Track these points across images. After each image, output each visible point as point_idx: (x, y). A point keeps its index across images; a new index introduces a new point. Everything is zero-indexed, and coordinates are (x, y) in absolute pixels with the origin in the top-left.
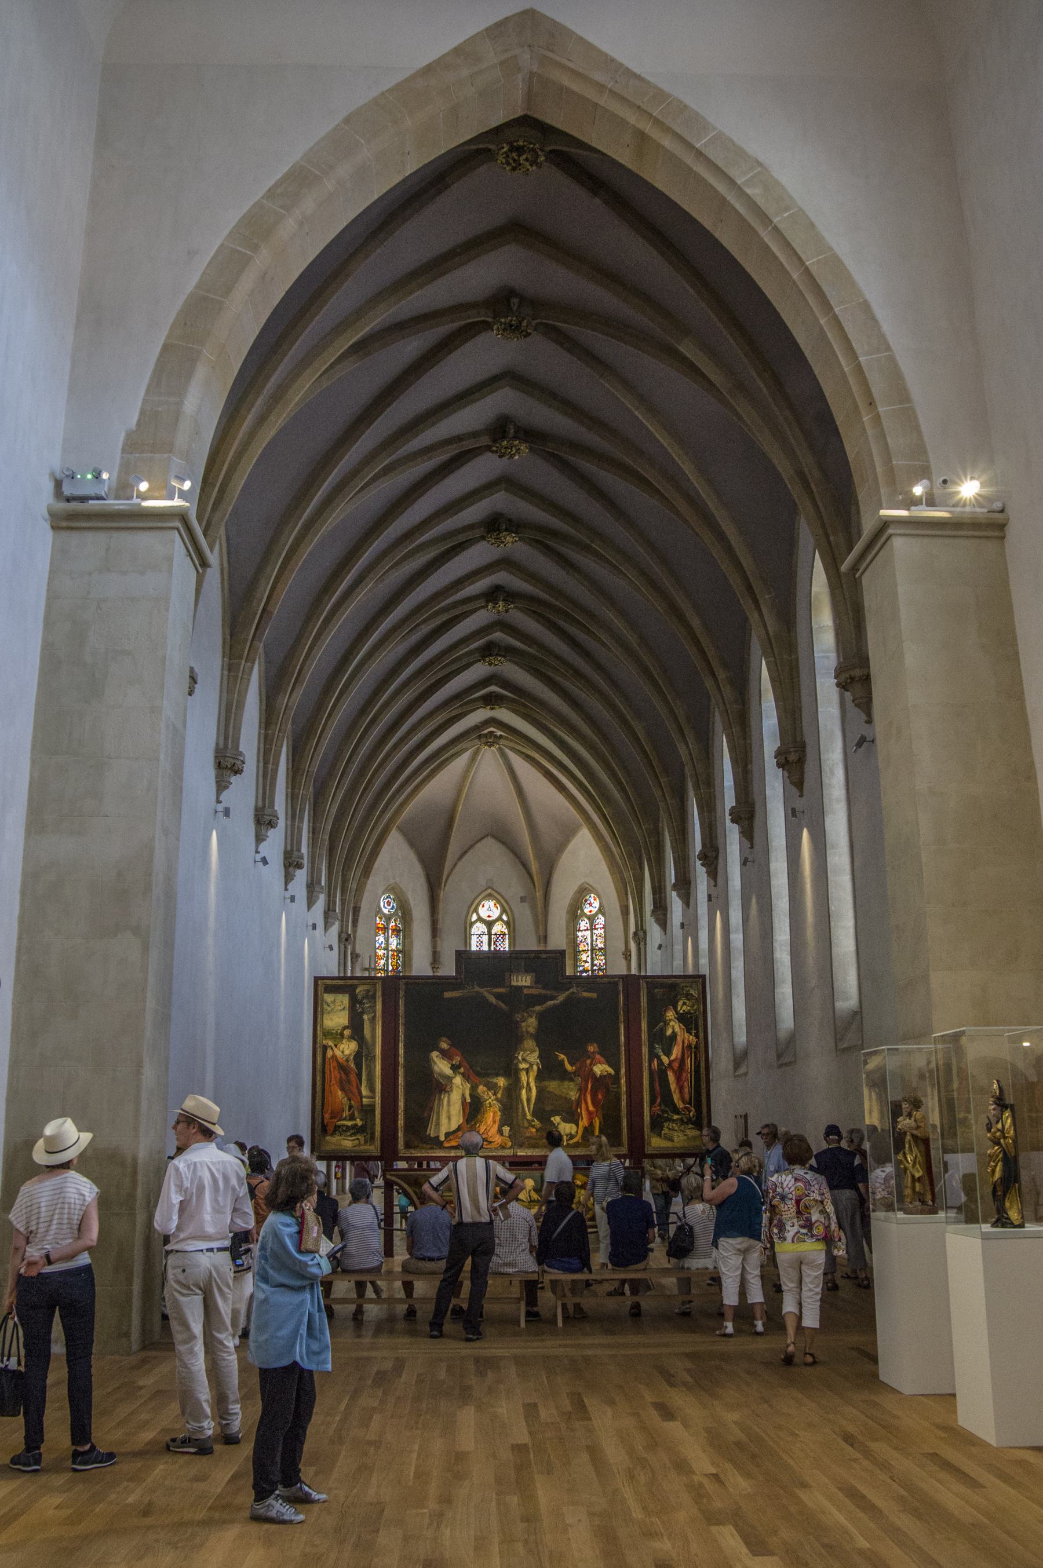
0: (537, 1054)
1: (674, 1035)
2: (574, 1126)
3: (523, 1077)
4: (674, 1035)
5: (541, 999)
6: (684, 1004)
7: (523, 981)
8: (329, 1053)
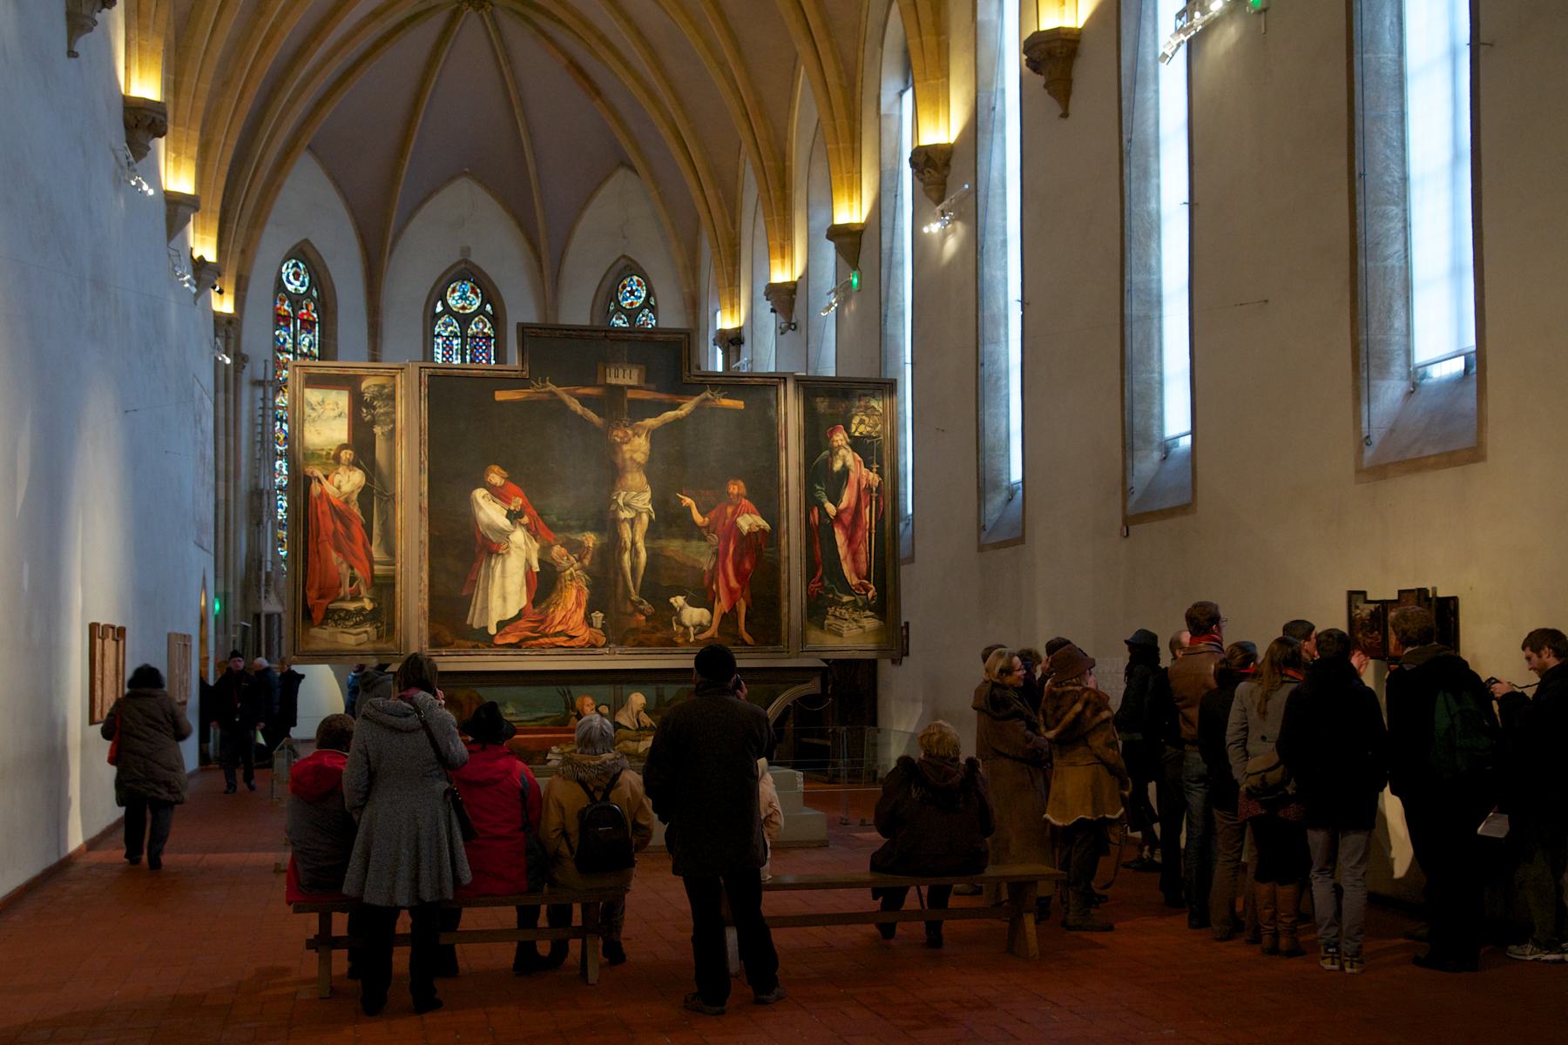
0: (648, 496)
1: (845, 471)
2: (705, 612)
4: (845, 471)
5: (657, 408)
6: (862, 422)
8: (315, 489)
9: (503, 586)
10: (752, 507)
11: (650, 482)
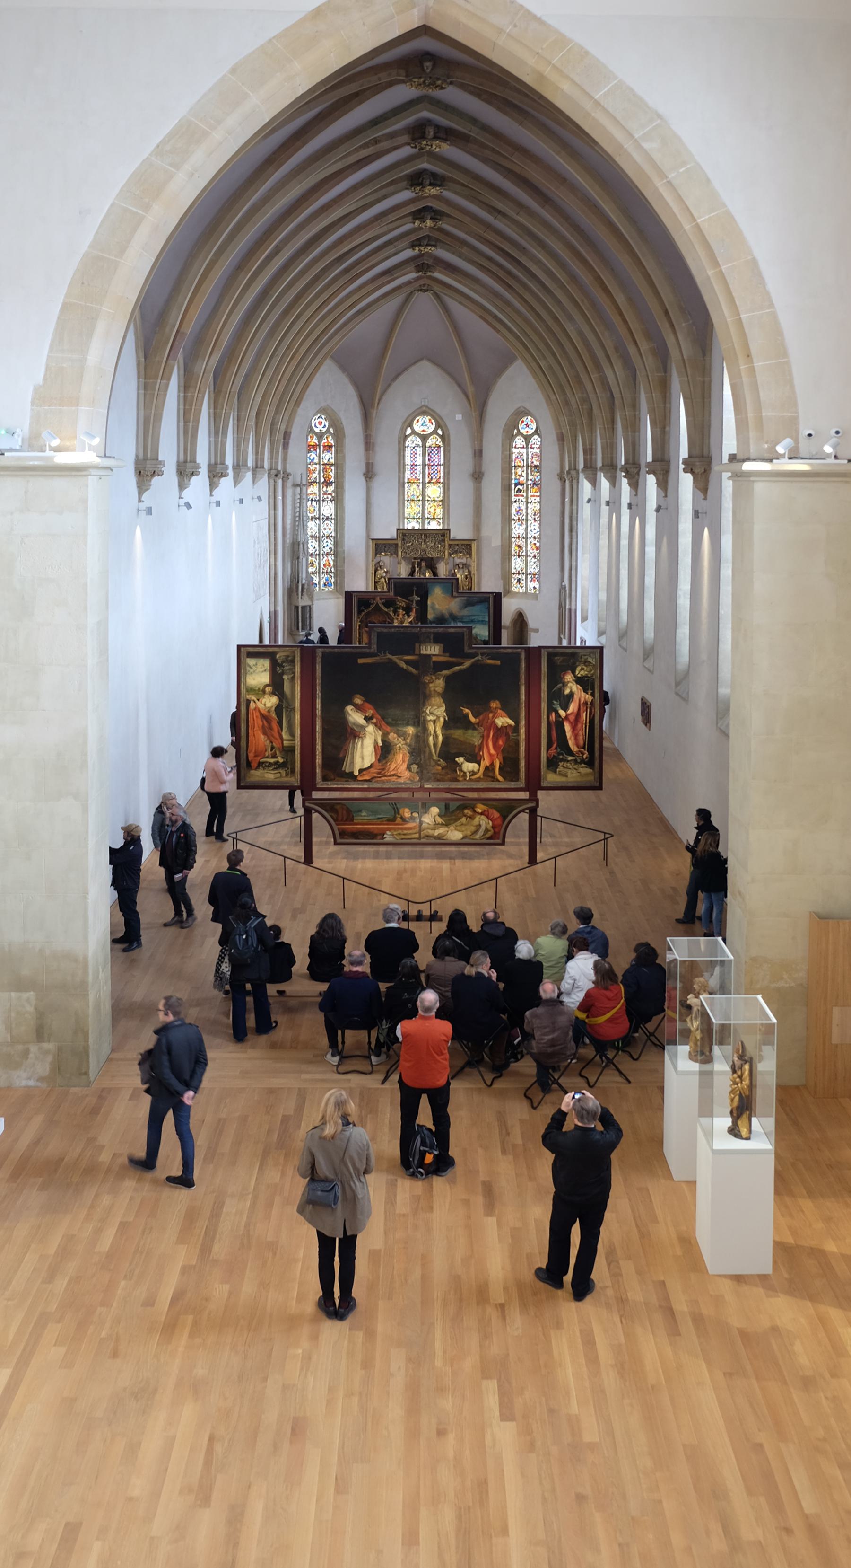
0: (443, 708)
3: (431, 727)
5: (448, 665)
7: (433, 650)
9: (362, 752)
10: (504, 714)
11: (444, 702)
